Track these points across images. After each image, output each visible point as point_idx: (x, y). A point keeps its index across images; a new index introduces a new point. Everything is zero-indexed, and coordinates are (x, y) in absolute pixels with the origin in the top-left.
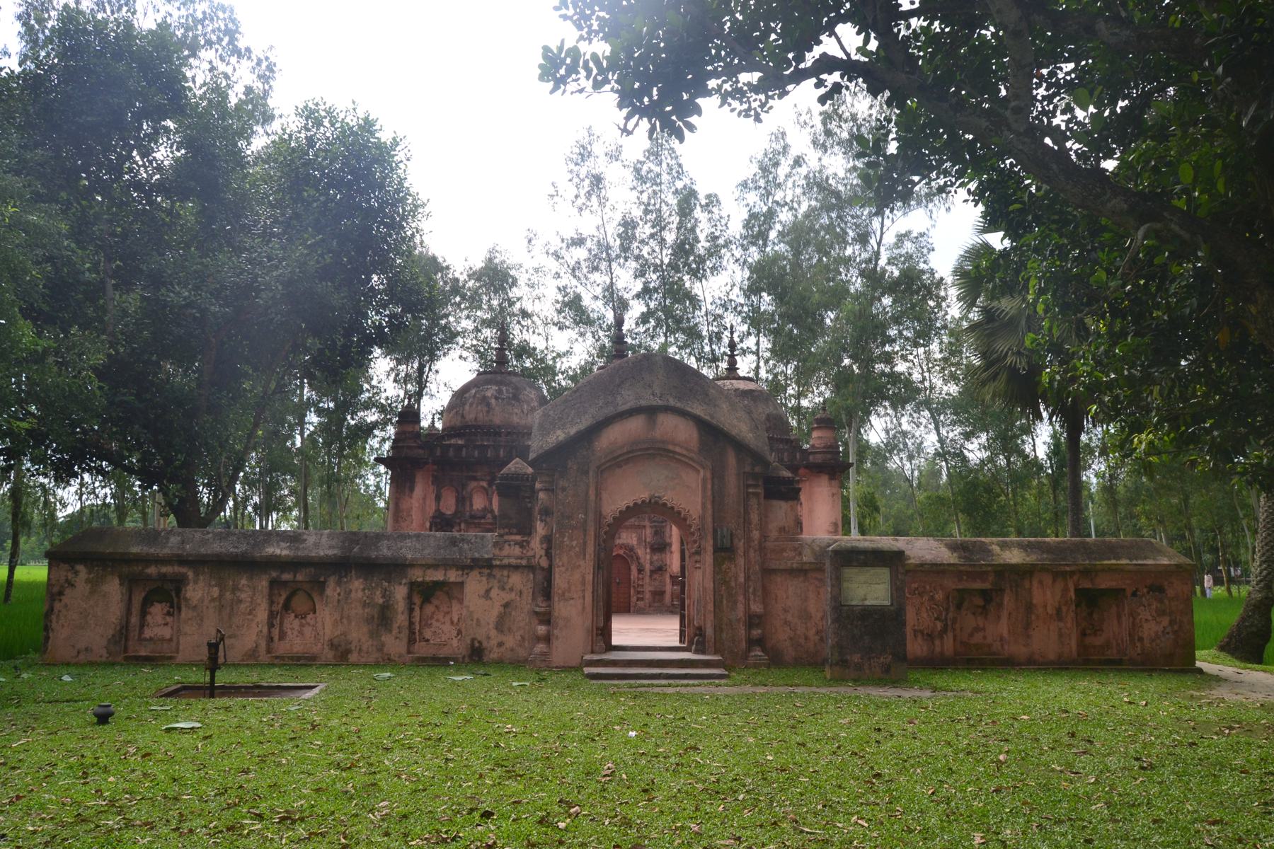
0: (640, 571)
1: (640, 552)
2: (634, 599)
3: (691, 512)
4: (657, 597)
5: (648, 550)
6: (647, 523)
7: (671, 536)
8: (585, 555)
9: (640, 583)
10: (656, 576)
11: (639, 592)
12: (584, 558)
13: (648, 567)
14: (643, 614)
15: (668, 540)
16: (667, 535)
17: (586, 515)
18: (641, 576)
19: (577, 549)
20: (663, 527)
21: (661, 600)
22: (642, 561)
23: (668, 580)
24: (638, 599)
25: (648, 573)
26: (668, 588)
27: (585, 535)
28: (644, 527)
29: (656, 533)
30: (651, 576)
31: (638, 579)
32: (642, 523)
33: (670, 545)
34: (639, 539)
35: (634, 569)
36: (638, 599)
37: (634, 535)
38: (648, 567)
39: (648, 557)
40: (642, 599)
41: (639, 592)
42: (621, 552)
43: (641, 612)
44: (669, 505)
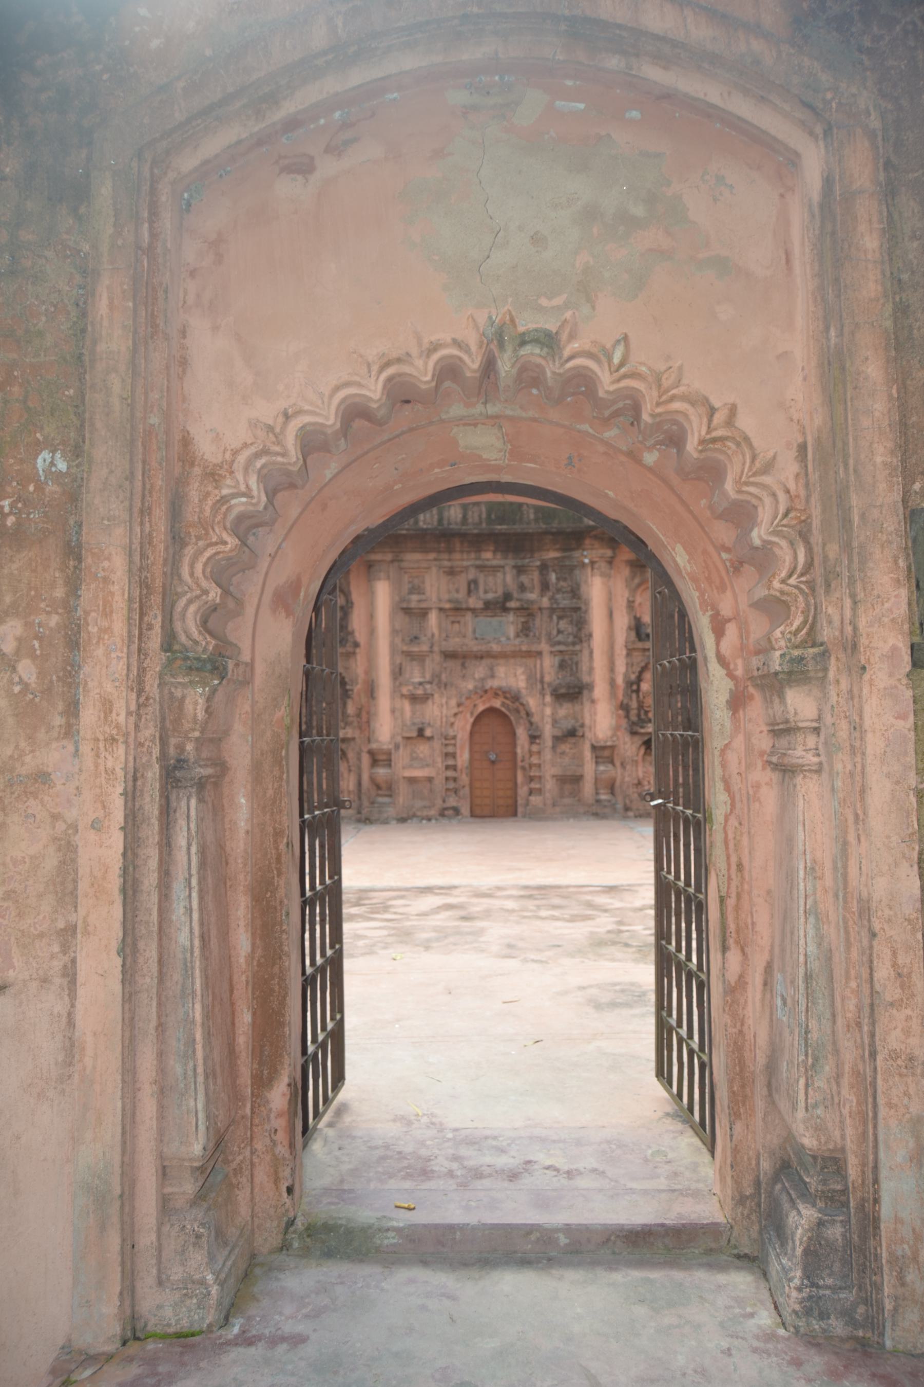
0: (534, 738)
1: (532, 703)
2: (523, 791)
3: (745, 422)
4: (568, 787)
5: (548, 699)
6: (544, 647)
7: (591, 670)
8: (72, 709)
9: (535, 760)
10: (564, 747)
11: (531, 779)
12: (69, 731)
13: (548, 731)
14: (546, 819)
15: (586, 679)
16: (584, 667)
17: (76, 452)
18: (535, 748)
19: (27, 670)
20: (574, 653)
21: (576, 794)
22: (535, 719)
23: (588, 754)
24: (531, 792)
25: (549, 743)
26: (589, 769)
27: (74, 587)
28: (540, 654)
29: (562, 666)
30: (554, 748)
31: (531, 753)
32: (534, 648)
33: (590, 687)
34: (530, 678)
35: (522, 733)
36: (531, 792)
37: (520, 671)
38: (548, 731)
39: (548, 711)
40: (540, 791)
41: (531, 779)
42: (497, 703)
43: (537, 816)
44: (606, 383)
